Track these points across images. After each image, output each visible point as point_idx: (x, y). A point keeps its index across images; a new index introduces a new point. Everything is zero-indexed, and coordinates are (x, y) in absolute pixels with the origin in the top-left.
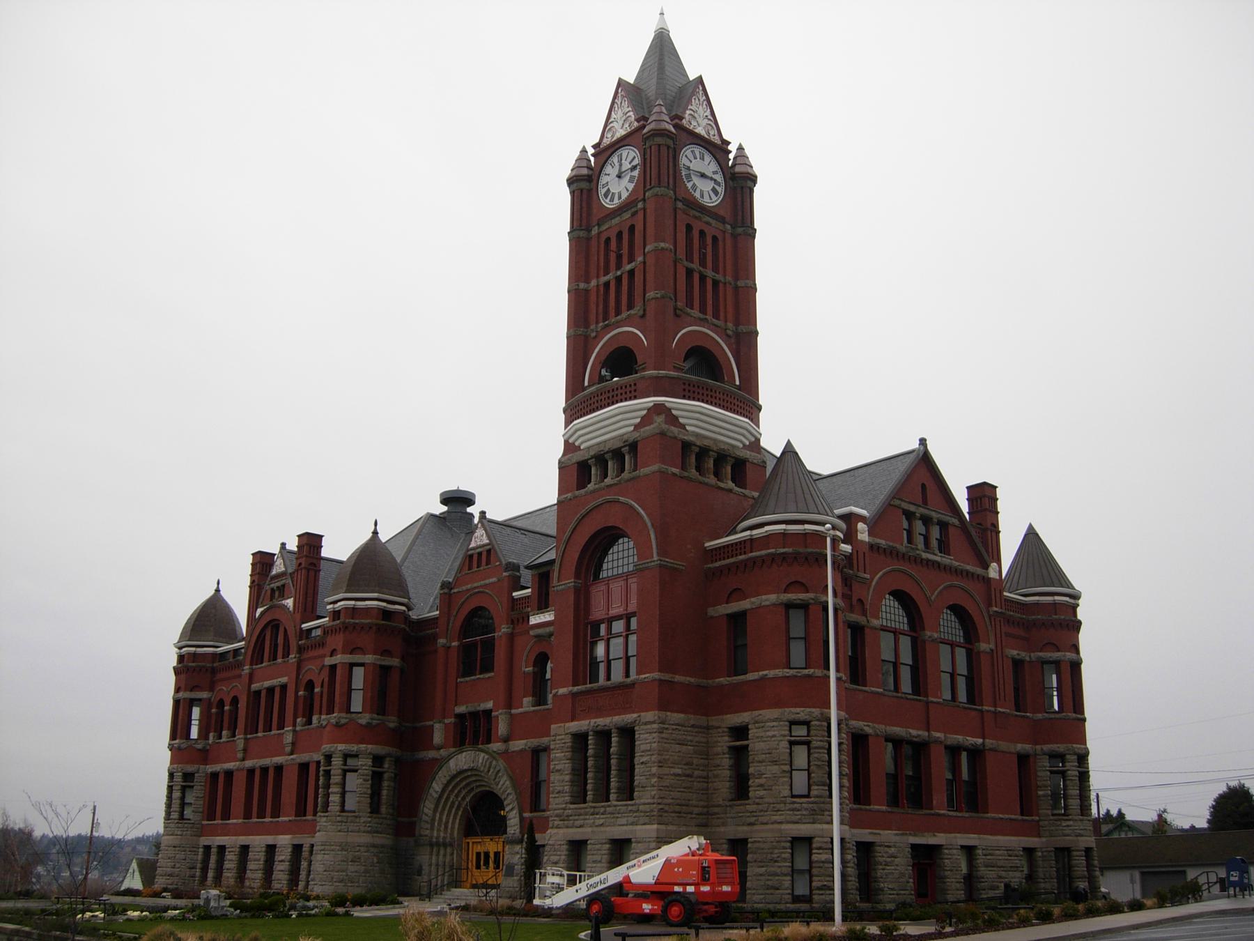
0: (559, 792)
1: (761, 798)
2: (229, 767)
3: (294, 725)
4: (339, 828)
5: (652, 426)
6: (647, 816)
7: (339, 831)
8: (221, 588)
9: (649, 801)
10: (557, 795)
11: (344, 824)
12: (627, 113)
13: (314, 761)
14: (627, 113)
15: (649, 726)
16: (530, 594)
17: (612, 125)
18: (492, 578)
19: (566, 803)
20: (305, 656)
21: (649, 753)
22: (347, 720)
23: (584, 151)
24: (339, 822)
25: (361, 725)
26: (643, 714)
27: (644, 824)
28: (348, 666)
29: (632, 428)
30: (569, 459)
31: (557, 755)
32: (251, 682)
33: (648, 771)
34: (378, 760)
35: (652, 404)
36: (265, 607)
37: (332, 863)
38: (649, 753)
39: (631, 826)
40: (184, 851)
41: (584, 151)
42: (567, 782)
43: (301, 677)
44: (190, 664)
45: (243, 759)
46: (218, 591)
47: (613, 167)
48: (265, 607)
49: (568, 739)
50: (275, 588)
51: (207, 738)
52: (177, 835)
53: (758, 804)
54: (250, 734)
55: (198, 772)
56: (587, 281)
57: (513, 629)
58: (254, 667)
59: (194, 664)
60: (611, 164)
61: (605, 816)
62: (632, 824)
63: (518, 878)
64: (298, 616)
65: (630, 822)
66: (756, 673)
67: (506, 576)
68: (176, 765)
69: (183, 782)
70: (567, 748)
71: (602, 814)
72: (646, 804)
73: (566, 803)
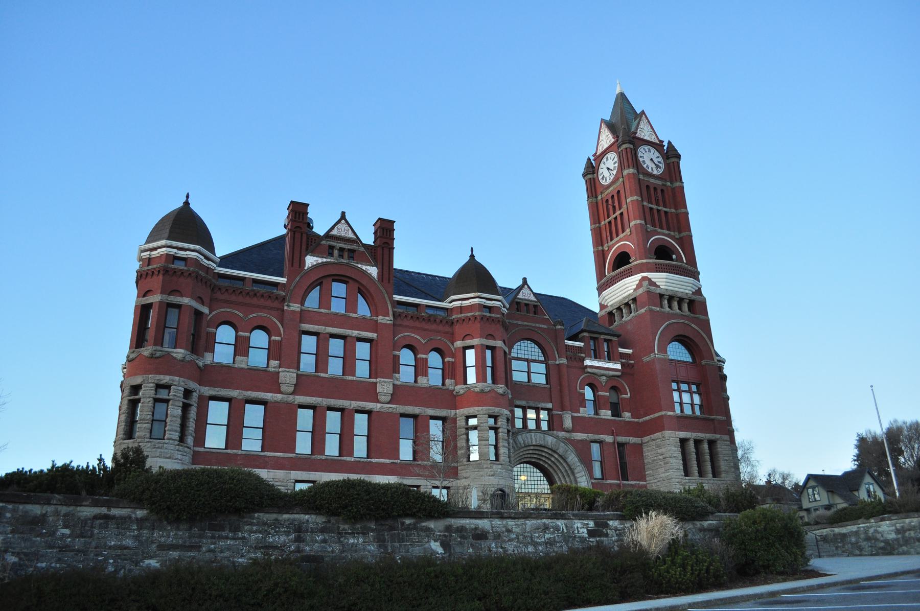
2: (265, 397)
13: (427, 416)
15: (726, 442)
28: (462, 350)
36: (325, 260)
45: (293, 393)
46: (187, 203)
48: (325, 260)
49: (678, 440)
52: (177, 459)
68: (177, 378)
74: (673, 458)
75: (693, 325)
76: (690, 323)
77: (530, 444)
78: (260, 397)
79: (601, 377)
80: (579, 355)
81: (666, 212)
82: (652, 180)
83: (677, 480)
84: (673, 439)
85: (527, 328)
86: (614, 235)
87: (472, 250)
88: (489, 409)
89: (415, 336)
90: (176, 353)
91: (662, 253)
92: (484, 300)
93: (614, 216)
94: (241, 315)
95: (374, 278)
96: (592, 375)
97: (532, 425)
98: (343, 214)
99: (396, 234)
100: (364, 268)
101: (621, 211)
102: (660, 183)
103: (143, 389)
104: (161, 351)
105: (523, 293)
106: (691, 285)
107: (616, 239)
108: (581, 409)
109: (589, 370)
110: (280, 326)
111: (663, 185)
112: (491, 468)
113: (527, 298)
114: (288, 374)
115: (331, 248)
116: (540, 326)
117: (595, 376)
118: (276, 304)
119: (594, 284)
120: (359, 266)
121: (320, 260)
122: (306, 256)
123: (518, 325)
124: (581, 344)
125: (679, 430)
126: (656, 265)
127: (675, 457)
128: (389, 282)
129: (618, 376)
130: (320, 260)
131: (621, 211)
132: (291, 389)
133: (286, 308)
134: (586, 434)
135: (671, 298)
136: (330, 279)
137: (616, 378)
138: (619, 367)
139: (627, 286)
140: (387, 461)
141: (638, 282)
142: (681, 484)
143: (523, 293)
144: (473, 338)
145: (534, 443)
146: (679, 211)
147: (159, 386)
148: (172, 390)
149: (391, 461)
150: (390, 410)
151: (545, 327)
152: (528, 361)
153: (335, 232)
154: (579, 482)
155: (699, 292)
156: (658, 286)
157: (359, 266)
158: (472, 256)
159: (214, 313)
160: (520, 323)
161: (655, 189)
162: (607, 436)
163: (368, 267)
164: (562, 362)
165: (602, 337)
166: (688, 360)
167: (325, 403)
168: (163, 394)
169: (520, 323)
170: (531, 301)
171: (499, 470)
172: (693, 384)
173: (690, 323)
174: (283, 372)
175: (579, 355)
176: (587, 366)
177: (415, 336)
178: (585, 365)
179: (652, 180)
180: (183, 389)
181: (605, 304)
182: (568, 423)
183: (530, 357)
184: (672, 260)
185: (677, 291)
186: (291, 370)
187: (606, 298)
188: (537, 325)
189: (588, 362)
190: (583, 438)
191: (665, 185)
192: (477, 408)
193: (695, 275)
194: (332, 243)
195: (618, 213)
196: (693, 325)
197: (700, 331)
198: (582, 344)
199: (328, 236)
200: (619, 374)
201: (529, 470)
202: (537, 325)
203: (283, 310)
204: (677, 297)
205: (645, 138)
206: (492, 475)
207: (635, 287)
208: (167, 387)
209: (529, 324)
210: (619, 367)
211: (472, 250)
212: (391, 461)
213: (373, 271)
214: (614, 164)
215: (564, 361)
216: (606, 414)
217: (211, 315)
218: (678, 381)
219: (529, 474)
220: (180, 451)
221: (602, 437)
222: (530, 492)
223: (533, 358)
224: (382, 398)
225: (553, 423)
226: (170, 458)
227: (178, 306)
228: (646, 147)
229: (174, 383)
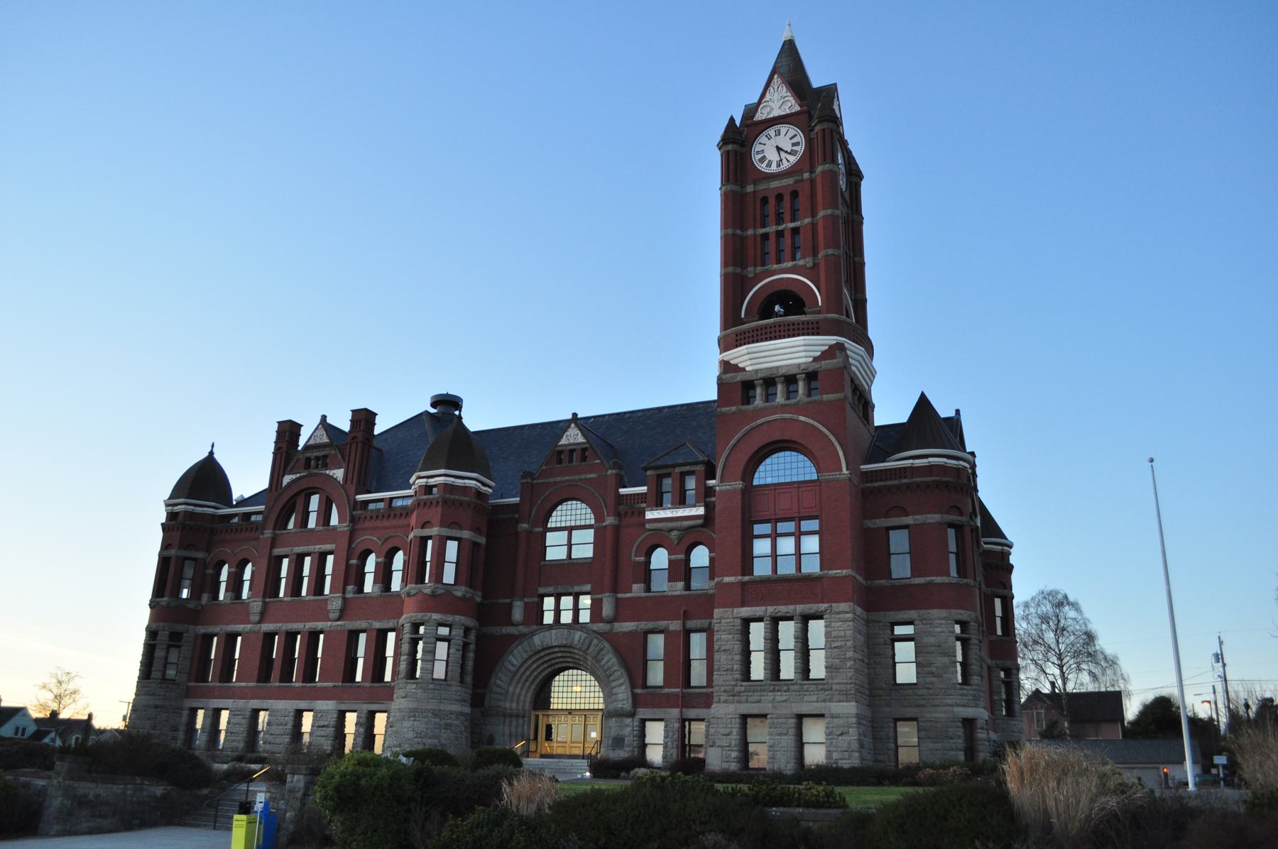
0: (727, 670)
1: (932, 683)
3: (344, 592)
4: (431, 696)
5: (835, 360)
6: (843, 694)
7: (432, 698)
8: (214, 450)
9: (844, 681)
10: (725, 673)
11: (436, 692)
12: (785, 97)
13: (374, 629)
14: (785, 97)
15: (842, 616)
16: (646, 491)
17: (765, 104)
18: (591, 473)
19: (737, 680)
20: (360, 526)
21: (843, 639)
22: (443, 591)
23: (732, 120)
24: (432, 689)
25: (457, 597)
26: (834, 605)
27: (839, 701)
29: (811, 359)
30: (732, 377)
31: (723, 637)
32: (273, 546)
33: (843, 655)
34: (467, 630)
35: (835, 342)
36: (298, 475)
37: (425, 730)
38: (843, 639)
39: (823, 703)
40: (167, 712)
41: (732, 120)
42: (737, 661)
43: (353, 546)
44: (187, 522)
45: (260, 622)
46: (211, 453)
47: (769, 139)
48: (298, 475)
50: (312, 457)
51: (199, 598)
52: (159, 696)
53: (929, 689)
54: (270, 598)
55: (187, 632)
56: (743, 229)
57: (620, 521)
58: (277, 532)
59: (192, 523)
60: (766, 136)
61: (788, 693)
62: (824, 701)
63: (630, 749)
64: (352, 488)
65: (819, 699)
66: (922, 579)
67: (611, 474)
69: (170, 641)
70: (737, 630)
71: (785, 691)
72: (840, 684)
73: (737, 680)
74: (723, 653)
75: (802, 418)
76: (795, 416)
77: (550, 645)
78: (234, 630)
79: (672, 533)
80: (638, 506)
82: (774, 184)
83: (722, 689)
84: (728, 620)
85: (567, 484)
88: (411, 617)
89: (372, 537)
92: (425, 480)
94: (230, 551)
95: (339, 482)
96: (658, 532)
97: (566, 618)
98: (324, 417)
102: (790, 181)
103: (159, 635)
105: (567, 436)
106: (802, 348)
108: (635, 587)
111: (796, 182)
112: (405, 688)
113: (572, 442)
114: (255, 603)
115: (308, 460)
116: (588, 476)
117: (664, 533)
120: (327, 472)
121: (294, 477)
122: (283, 477)
123: (556, 483)
125: (743, 605)
126: (737, 335)
127: (725, 650)
128: (352, 483)
130: (294, 477)
132: (257, 618)
133: (261, 537)
134: (637, 623)
135: (769, 382)
137: (700, 529)
140: (330, 684)
142: (731, 694)
143: (567, 436)
144: (432, 527)
145: (554, 644)
149: (333, 684)
150: (339, 628)
151: (593, 476)
152: (570, 529)
153: (311, 442)
154: (615, 694)
156: (743, 369)
157: (327, 472)
159: (212, 554)
160: (558, 479)
162: (670, 622)
163: (335, 471)
165: (678, 470)
166: (808, 478)
167: (283, 628)
169: (558, 479)
170: (578, 444)
171: (413, 691)
173: (795, 416)
174: (253, 602)
175: (638, 506)
177: (372, 537)
179: (774, 184)
180: (167, 633)
182: (607, 610)
183: (573, 524)
184: (777, 315)
185: (778, 368)
186: (257, 599)
188: (583, 477)
189: (650, 515)
190: (631, 629)
191: (802, 181)
194: (308, 455)
196: (802, 418)
197: (816, 424)
199: (307, 447)
200: (700, 522)
201: (584, 678)
202: (583, 477)
203: (258, 538)
204: (781, 376)
205: (771, 116)
206: (404, 697)
209: (572, 478)
212: (333, 684)
217: (210, 557)
218: (770, 519)
219: (583, 683)
220: (162, 688)
221: (662, 624)
222: (573, 708)
223: (578, 523)
224: (332, 616)
225: (596, 608)
226: (153, 695)
228: (771, 132)
229: (160, 629)
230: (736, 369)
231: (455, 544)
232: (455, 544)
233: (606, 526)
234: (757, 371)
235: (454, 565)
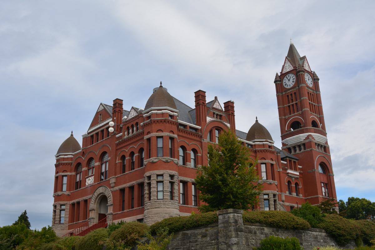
81: (314, 105)
82: (309, 90)
86: (292, 112)
87: (257, 118)
90: (175, 160)
91: (314, 124)
93: (292, 104)
99: (235, 109)
100: (226, 124)
101: (297, 102)
102: (312, 91)
104: (170, 159)
107: (292, 115)
109: (289, 175)
110: (201, 149)
115: (214, 113)
118: (198, 139)
119: (280, 134)
124: (285, 163)
129: (297, 178)
131: (297, 102)
133: (202, 141)
136: (215, 128)
138: (298, 174)
139: (301, 137)
141: (306, 136)
146: (319, 105)
147: (158, 175)
148: (164, 176)
155: (327, 143)
156: (315, 139)
157: (224, 123)
158: (257, 121)
161: (310, 94)
164: (281, 170)
165: (293, 160)
168: (160, 179)
172: (322, 183)
176: (288, 173)
178: (287, 172)
181: (286, 144)
187: (288, 141)
192: (269, 191)
193: (325, 134)
194: (215, 112)
195: (294, 103)
198: (286, 163)
200: (299, 177)
203: (201, 142)
207: (305, 138)
208: (162, 175)
210: (298, 174)
211: (257, 118)
213: (228, 125)
214: (293, 79)
215: (281, 170)
216: (294, 194)
227: (162, 137)
229: (176, 174)
230: (313, 138)
231: (264, 165)
232: (264, 165)
233: (279, 171)
234: (318, 141)
235: (265, 173)
